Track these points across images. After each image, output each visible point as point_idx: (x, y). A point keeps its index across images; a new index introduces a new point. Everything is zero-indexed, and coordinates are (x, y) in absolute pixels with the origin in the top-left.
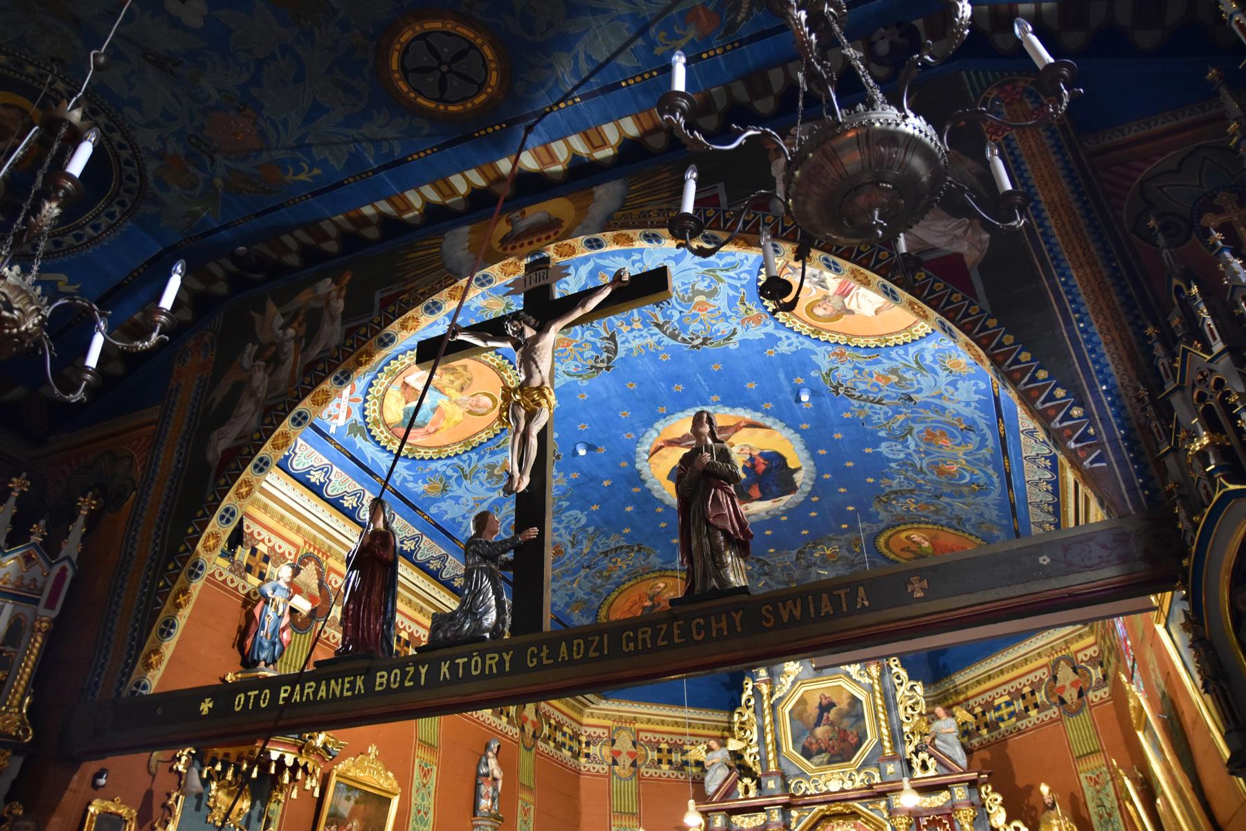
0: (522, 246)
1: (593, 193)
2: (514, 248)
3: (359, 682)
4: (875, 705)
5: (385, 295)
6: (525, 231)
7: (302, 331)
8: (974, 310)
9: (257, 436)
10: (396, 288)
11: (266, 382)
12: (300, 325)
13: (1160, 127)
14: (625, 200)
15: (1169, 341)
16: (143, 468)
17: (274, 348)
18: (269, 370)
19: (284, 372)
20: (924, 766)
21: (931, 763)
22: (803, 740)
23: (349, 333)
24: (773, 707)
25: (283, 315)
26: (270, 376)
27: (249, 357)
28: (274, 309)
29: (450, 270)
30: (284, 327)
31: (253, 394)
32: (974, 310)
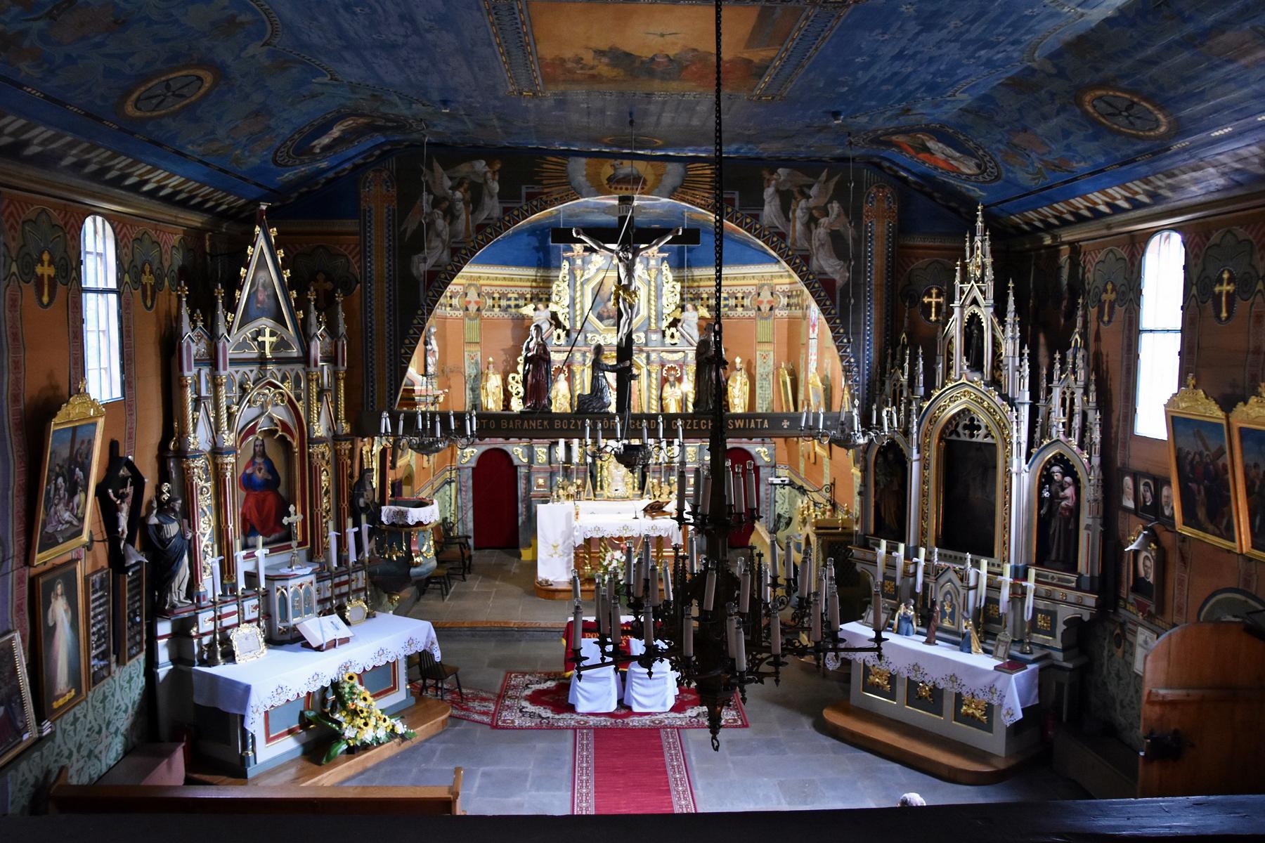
0: (621, 189)
1: (665, 167)
2: (616, 188)
3: (545, 423)
4: (649, 294)
5: (530, 190)
6: (624, 178)
7: (468, 196)
8: (833, 312)
9: (449, 268)
10: (537, 189)
11: (448, 229)
12: (466, 191)
13: (927, 243)
14: (684, 180)
15: (894, 358)
16: (359, 267)
17: (447, 203)
18: (448, 220)
19: (461, 224)
20: (672, 336)
21: (677, 335)
22: (599, 309)
23: (506, 211)
24: (582, 284)
25: (451, 178)
26: (450, 224)
27: (427, 203)
28: (441, 170)
29: (574, 189)
30: (453, 188)
31: (438, 235)
32: (833, 312)
